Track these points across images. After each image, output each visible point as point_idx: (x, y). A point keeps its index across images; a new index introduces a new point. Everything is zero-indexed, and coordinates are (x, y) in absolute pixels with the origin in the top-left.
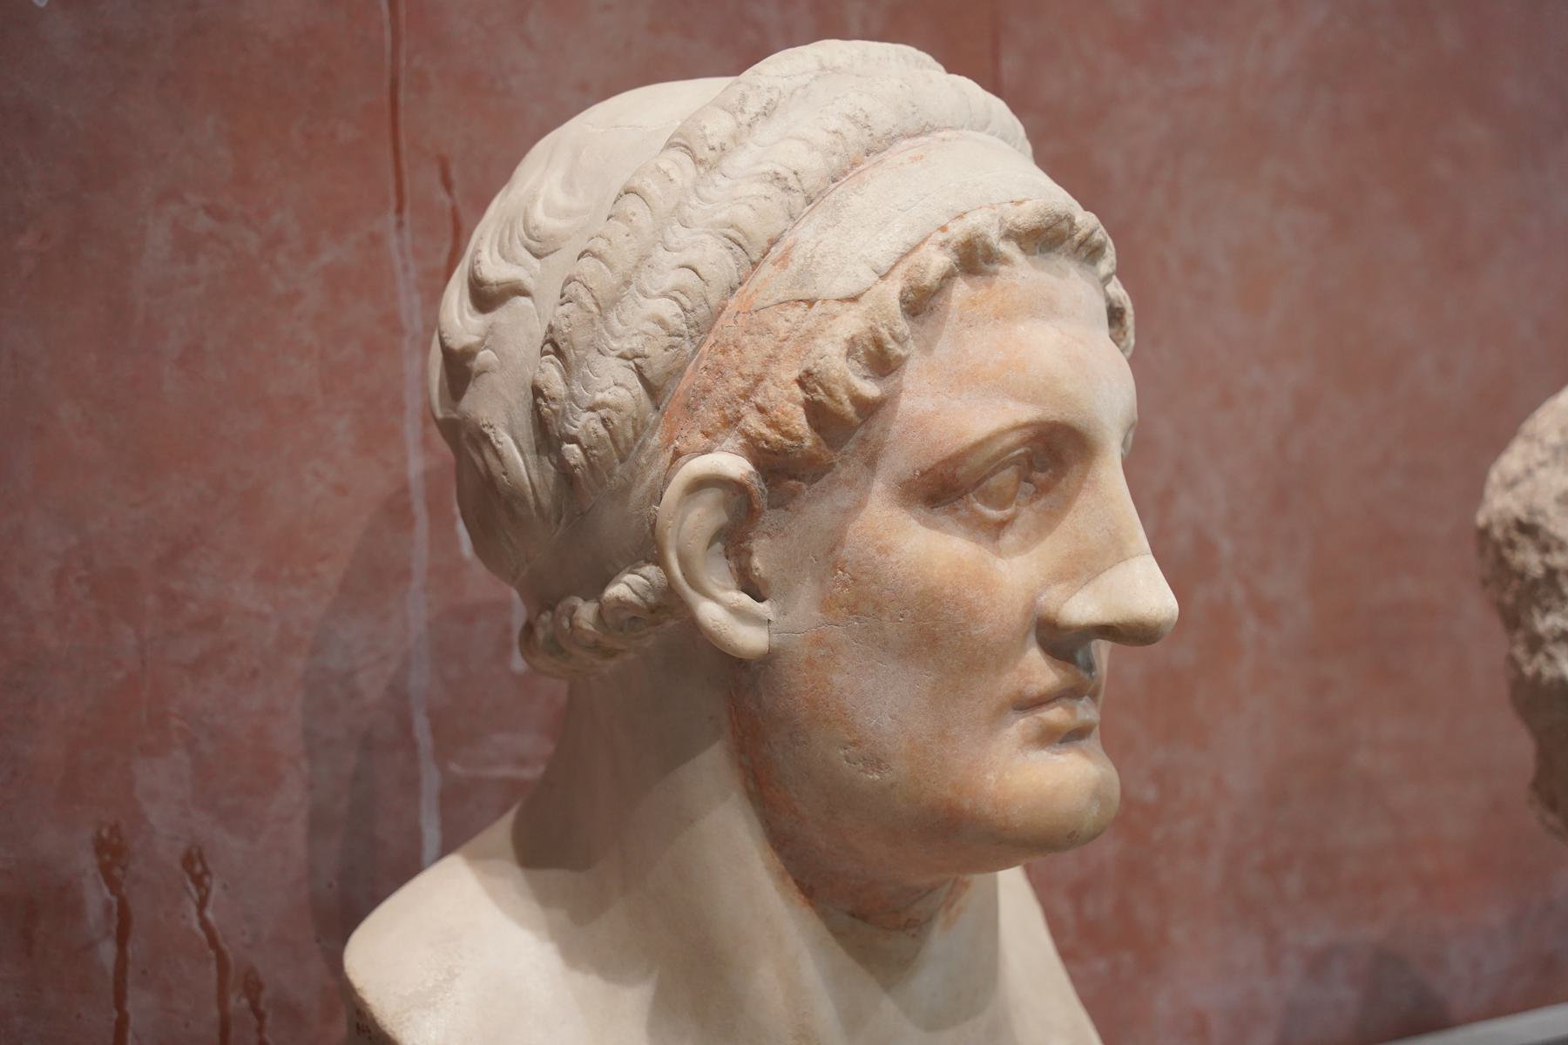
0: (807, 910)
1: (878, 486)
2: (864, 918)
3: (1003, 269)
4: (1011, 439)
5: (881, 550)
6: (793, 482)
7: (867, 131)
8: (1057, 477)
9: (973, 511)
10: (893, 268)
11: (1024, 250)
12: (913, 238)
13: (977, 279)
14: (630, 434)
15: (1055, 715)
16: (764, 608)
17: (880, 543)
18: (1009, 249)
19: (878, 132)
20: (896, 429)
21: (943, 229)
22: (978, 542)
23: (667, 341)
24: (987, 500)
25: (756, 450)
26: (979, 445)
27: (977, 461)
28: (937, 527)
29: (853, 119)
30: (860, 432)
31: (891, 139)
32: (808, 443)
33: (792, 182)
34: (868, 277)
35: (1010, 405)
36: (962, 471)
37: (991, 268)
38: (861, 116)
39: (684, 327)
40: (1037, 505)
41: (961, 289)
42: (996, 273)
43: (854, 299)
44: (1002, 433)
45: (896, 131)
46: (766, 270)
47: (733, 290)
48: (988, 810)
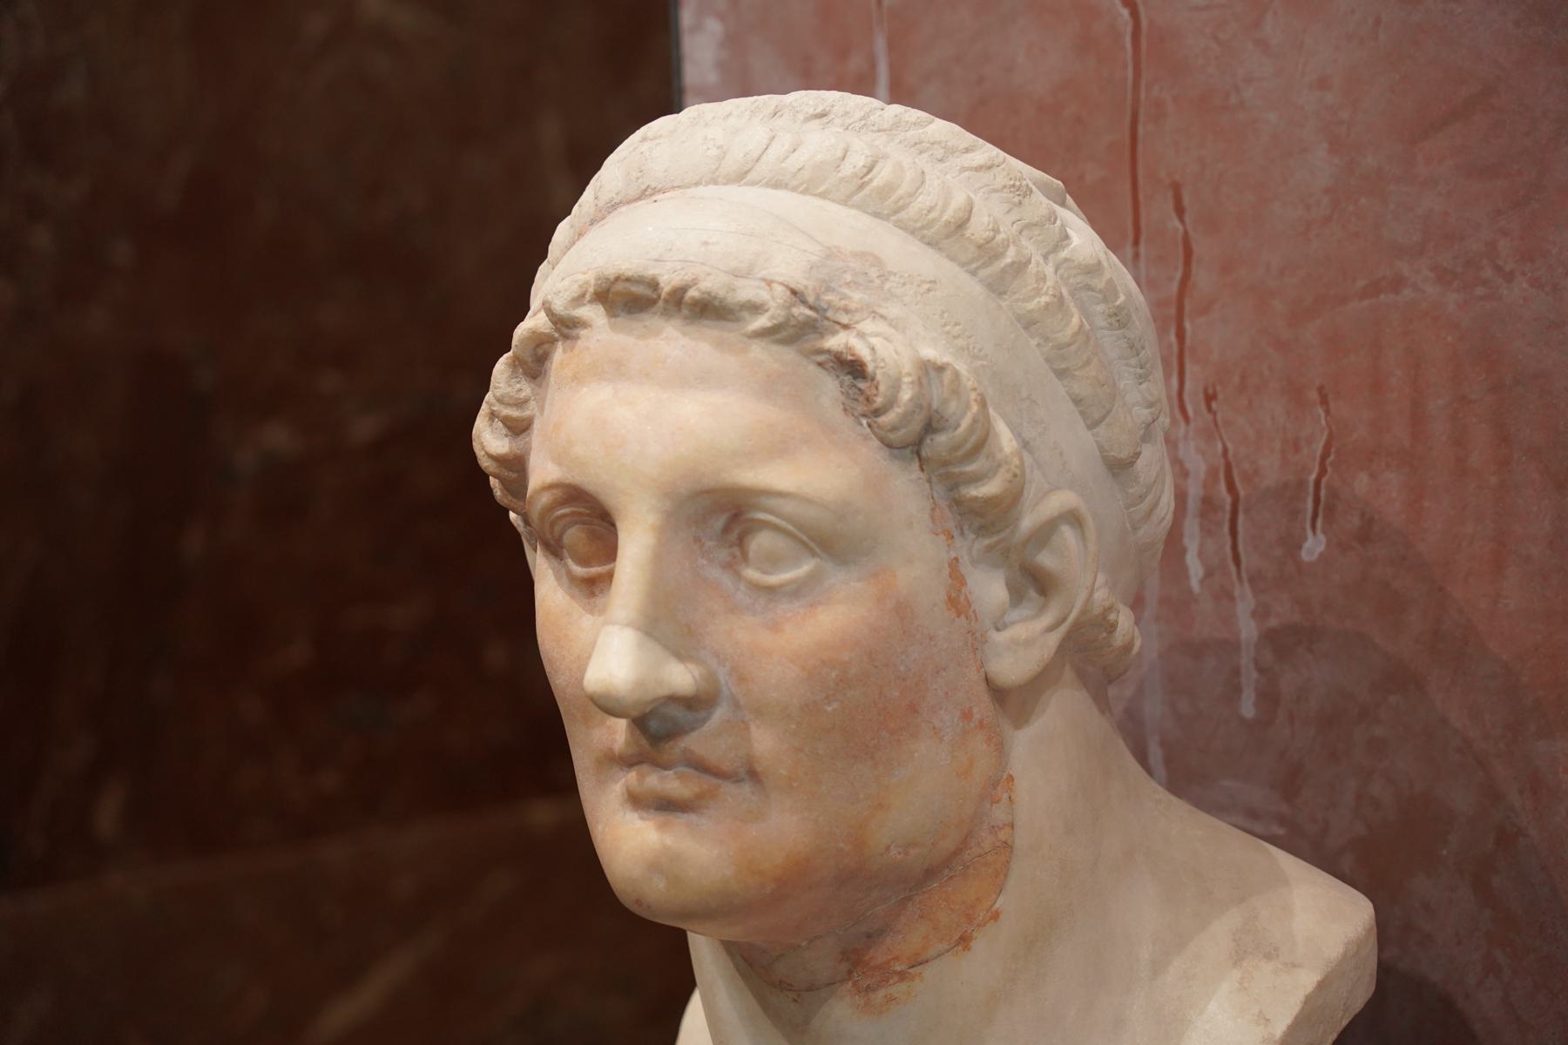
3: (583, 332)
18: (593, 313)
22: (573, 597)
37: (574, 332)
42: (578, 338)
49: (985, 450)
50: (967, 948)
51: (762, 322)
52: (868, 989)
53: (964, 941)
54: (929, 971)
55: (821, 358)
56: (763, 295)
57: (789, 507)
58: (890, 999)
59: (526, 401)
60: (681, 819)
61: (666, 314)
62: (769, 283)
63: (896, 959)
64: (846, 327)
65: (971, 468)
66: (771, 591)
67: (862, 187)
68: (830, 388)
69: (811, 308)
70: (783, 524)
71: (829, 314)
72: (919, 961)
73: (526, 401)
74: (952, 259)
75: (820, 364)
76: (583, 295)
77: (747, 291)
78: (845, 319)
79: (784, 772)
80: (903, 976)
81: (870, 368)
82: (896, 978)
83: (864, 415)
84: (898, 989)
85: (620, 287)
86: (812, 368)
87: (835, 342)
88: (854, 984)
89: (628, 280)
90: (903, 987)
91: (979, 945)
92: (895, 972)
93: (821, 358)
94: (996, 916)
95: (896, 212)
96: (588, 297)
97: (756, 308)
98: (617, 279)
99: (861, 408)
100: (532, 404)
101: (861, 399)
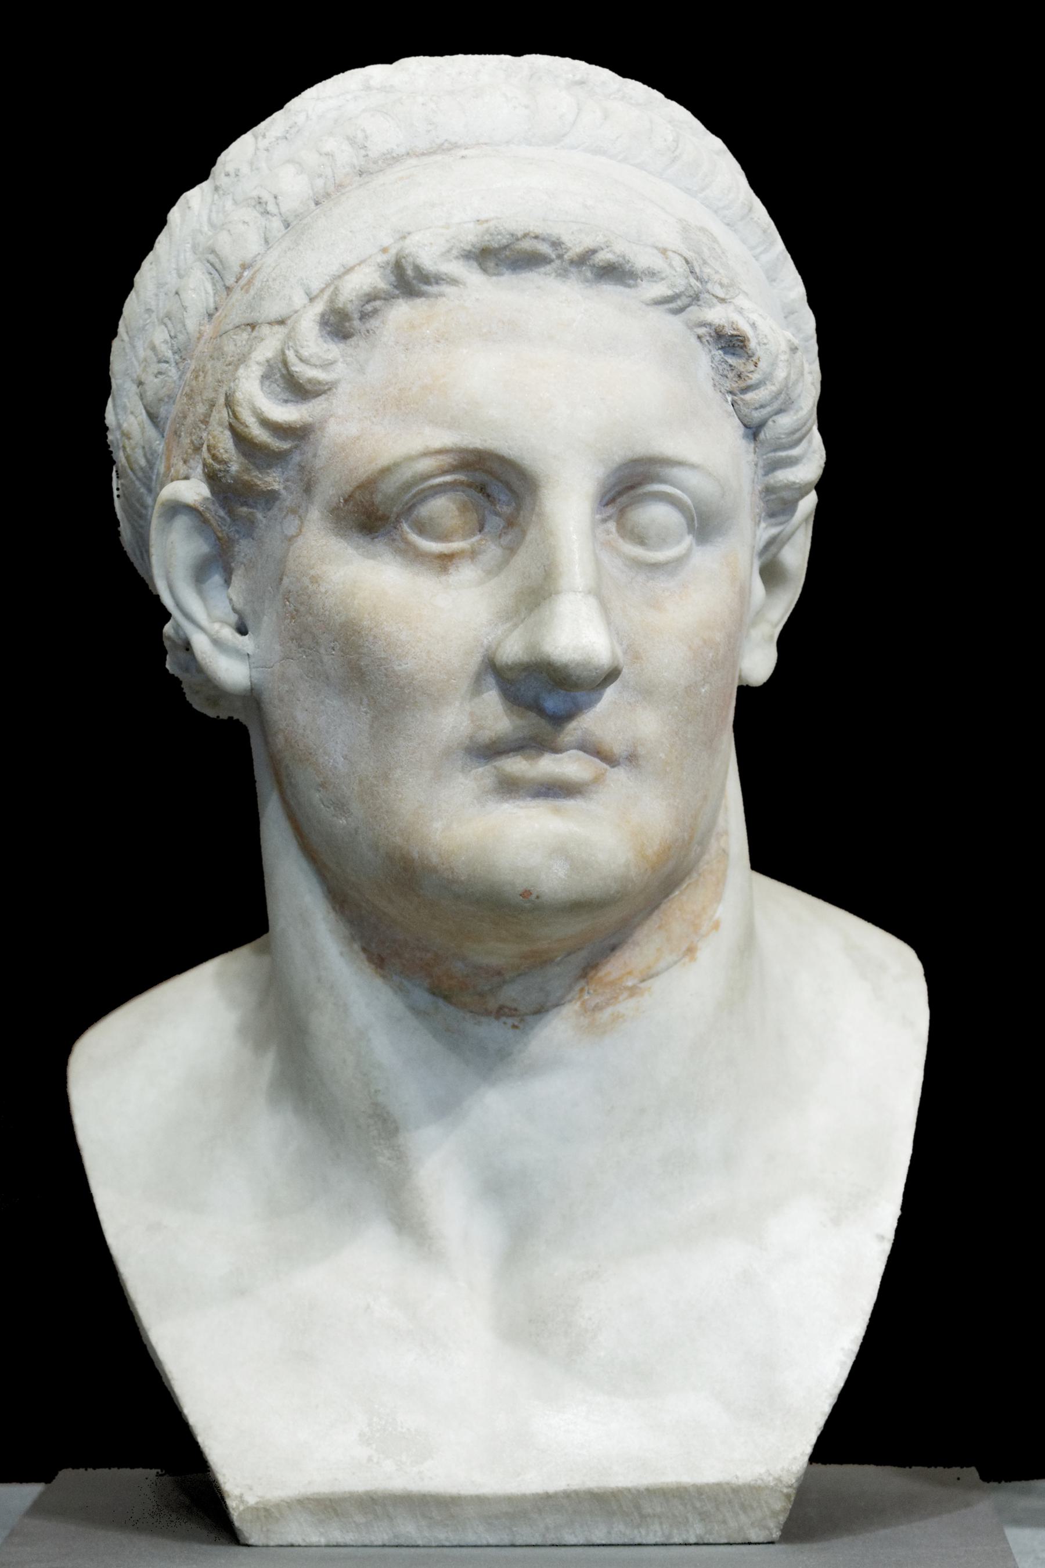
0: (378, 982)
1: (315, 514)
2: (447, 998)
3: (445, 288)
4: (425, 465)
5: (314, 580)
6: (245, 509)
7: (363, 152)
8: (518, 508)
9: (407, 543)
10: (322, 291)
11: (485, 270)
12: (350, 260)
13: (419, 301)
14: (143, 462)
15: (516, 765)
16: (245, 643)
17: (312, 572)
18: (455, 268)
19: (374, 153)
20: (323, 453)
21: (385, 250)
23: (155, 367)
24: (422, 528)
25: (212, 478)
26: (386, 471)
27: (390, 486)
28: (373, 557)
29: (352, 141)
30: (296, 458)
31: (392, 159)
32: (234, 468)
33: (271, 208)
34: (299, 299)
35: (427, 430)
36: (378, 498)
38: (360, 135)
39: (169, 354)
40: (505, 540)
41: (402, 311)
42: (442, 295)
43: (282, 322)
44: (410, 459)
45: (402, 150)
46: (237, 295)
47: (210, 316)
48: (435, 859)
49: (808, 437)
50: (693, 959)
51: (659, 290)
52: (598, 1008)
53: (691, 951)
54: (656, 984)
55: (702, 331)
56: (656, 262)
57: (691, 479)
58: (617, 1018)
59: (332, 363)
60: (570, 803)
61: (563, 274)
62: (664, 251)
63: (630, 973)
64: (723, 300)
65: (795, 452)
66: (655, 567)
67: (674, 160)
68: (704, 361)
69: (697, 279)
70: (685, 498)
71: (709, 286)
72: (648, 976)
73: (332, 363)
74: (744, 241)
75: (699, 337)
76: (449, 251)
77: (643, 259)
78: (721, 294)
79: (662, 755)
80: (633, 991)
81: (753, 344)
82: (626, 994)
83: (731, 393)
84: (626, 1006)
85: (526, 245)
86: (694, 340)
87: (717, 315)
88: (583, 1004)
89: (536, 237)
90: (632, 1003)
91: (705, 954)
92: (627, 988)
93: (702, 331)
94: (716, 926)
95: (703, 189)
96: (455, 252)
97: (652, 275)
98: (525, 236)
99: (728, 385)
100: (340, 366)
101: (731, 375)
